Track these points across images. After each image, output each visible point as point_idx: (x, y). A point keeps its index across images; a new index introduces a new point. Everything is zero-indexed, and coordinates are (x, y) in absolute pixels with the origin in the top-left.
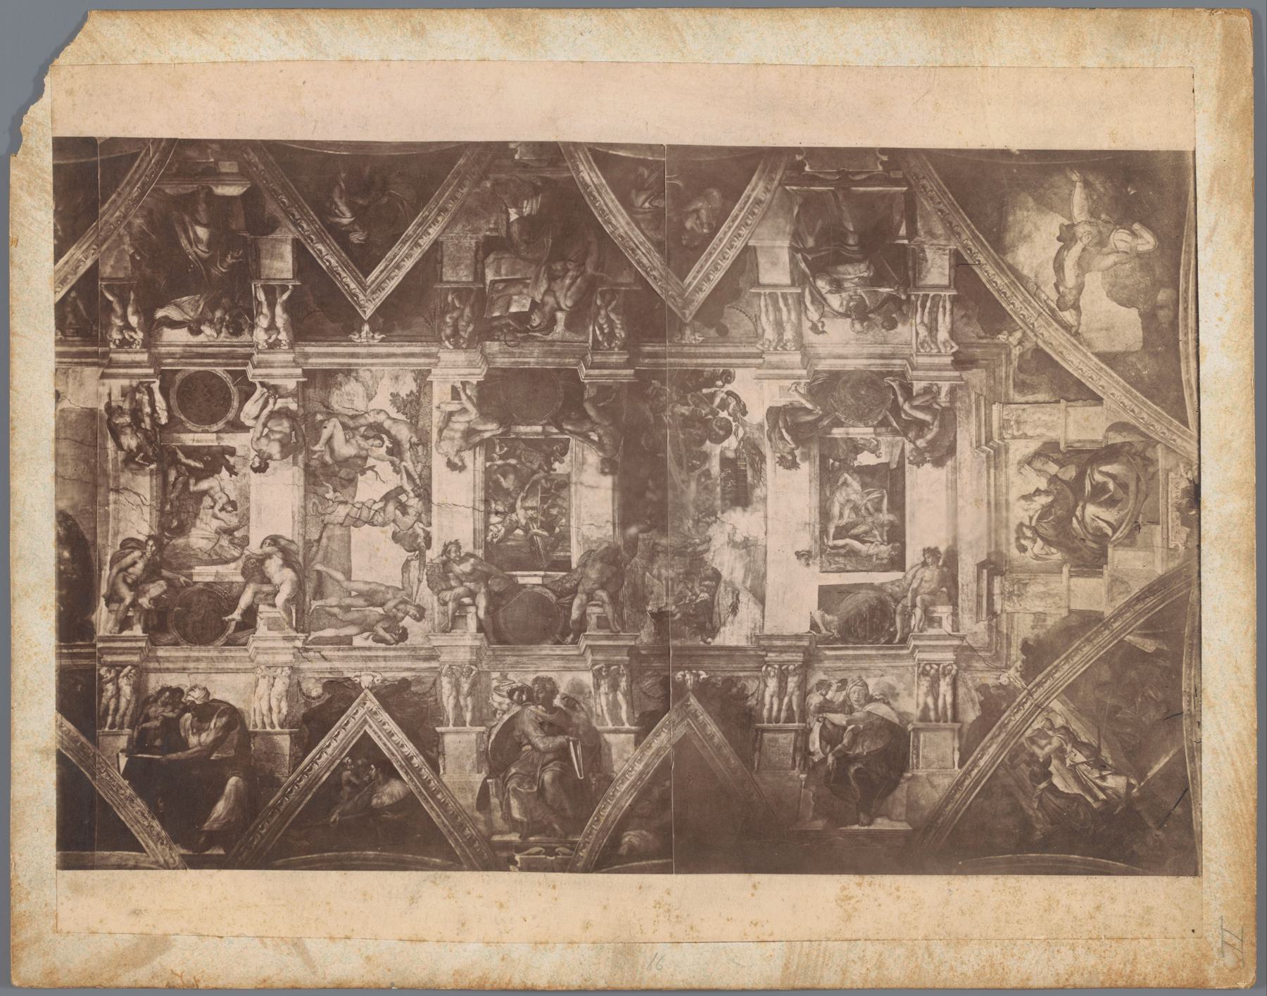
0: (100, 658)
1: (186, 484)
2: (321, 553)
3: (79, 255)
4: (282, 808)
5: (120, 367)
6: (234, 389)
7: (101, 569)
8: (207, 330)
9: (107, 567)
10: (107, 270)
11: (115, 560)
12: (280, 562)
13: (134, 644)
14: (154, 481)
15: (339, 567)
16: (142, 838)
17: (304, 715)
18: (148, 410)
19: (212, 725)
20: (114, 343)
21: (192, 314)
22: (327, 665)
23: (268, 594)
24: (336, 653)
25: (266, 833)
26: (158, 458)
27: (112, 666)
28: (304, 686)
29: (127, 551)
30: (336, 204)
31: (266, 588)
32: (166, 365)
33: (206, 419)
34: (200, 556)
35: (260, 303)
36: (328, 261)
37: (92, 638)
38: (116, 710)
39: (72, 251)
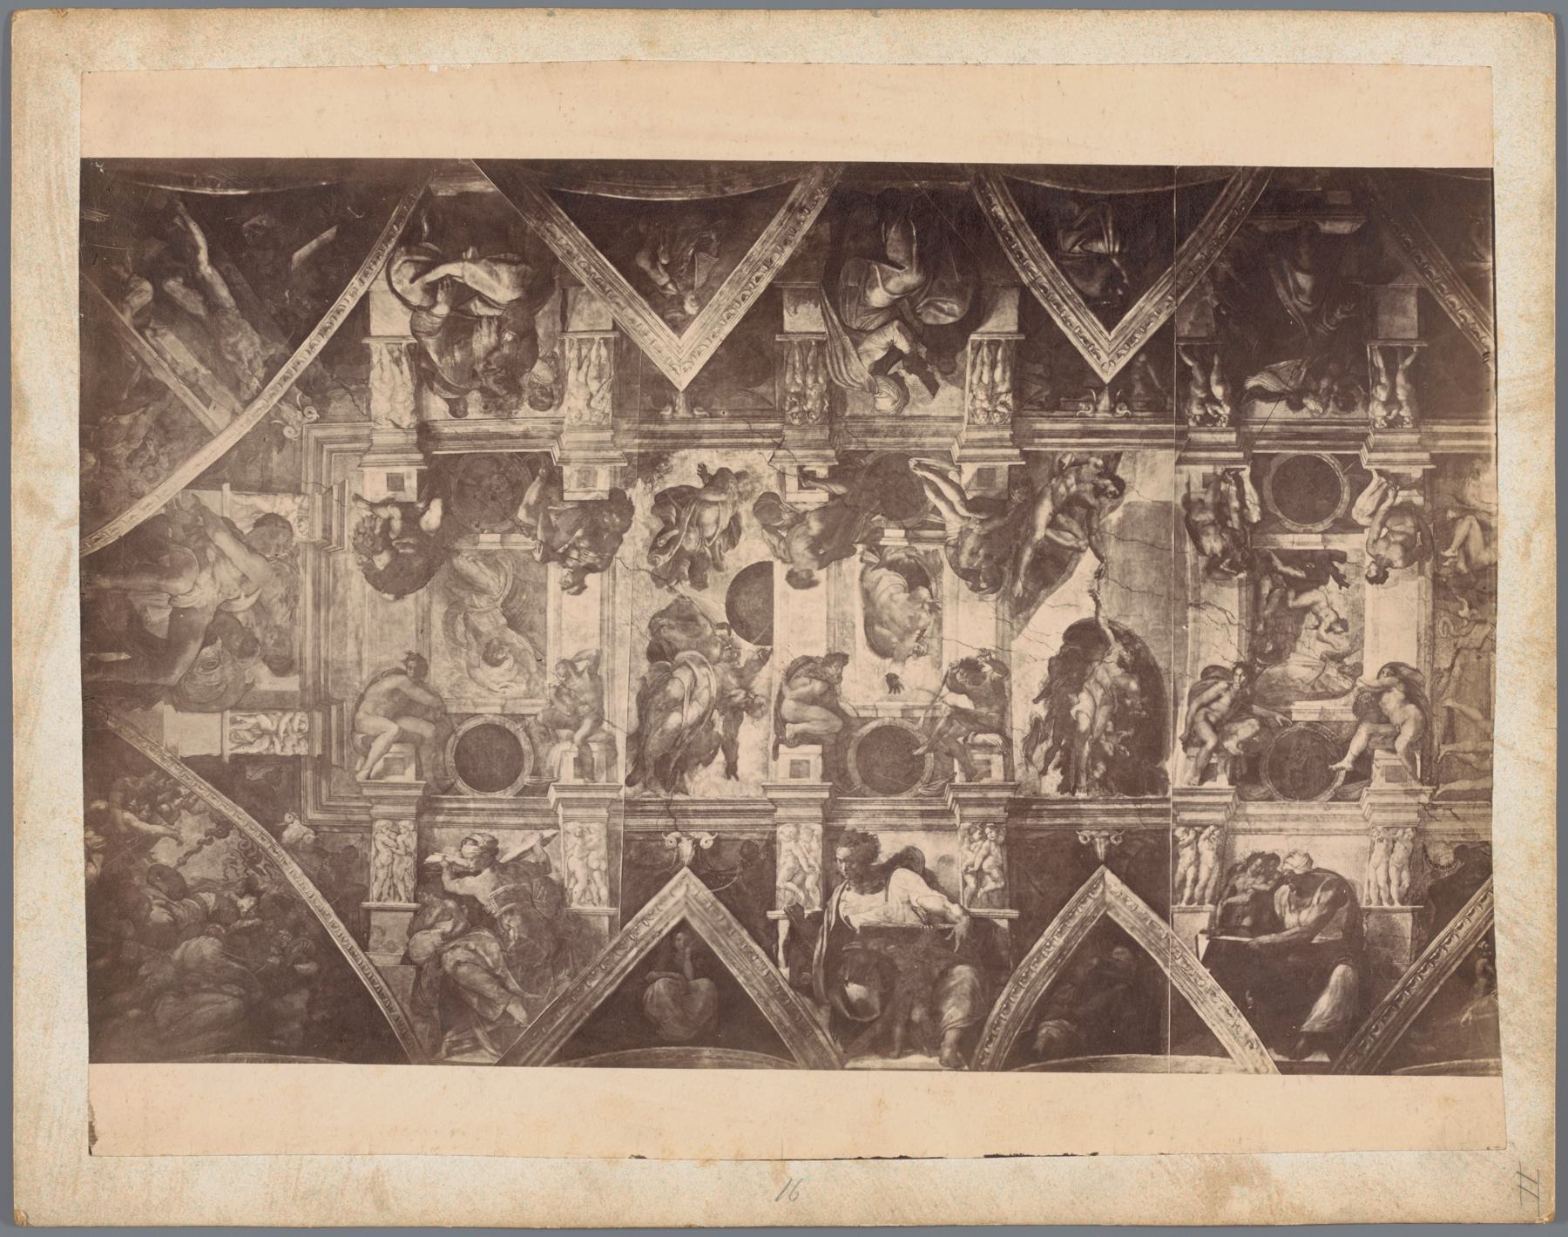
0: (1174, 816)
1: (1284, 599)
2: (1452, 686)
3: (1149, 308)
4: (1401, 1004)
5: (1200, 450)
6: (1344, 479)
7: (1176, 705)
8: (1311, 404)
9: (1185, 701)
10: (1185, 329)
11: (1194, 694)
12: (1402, 696)
13: (1217, 799)
14: (1244, 594)
15: (1475, 704)
16: (1225, 1039)
17: (1430, 888)
18: (1235, 504)
19: (1315, 900)
20: (1194, 420)
21: (1292, 383)
22: (1459, 826)
23: (1386, 737)
24: (1471, 811)
25: (1380, 1036)
26: (1249, 565)
27: (1189, 825)
28: (1431, 852)
29: (1209, 682)
30: (1474, 244)
31: (1384, 729)
32: (1259, 447)
33: (1307, 517)
34: (1301, 688)
35: (1377, 370)
36: (1463, 316)
37: (1166, 792)
38: (1196, 881)
39: (1140, 303)
